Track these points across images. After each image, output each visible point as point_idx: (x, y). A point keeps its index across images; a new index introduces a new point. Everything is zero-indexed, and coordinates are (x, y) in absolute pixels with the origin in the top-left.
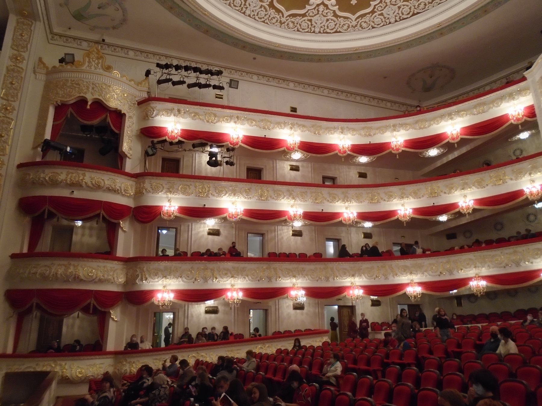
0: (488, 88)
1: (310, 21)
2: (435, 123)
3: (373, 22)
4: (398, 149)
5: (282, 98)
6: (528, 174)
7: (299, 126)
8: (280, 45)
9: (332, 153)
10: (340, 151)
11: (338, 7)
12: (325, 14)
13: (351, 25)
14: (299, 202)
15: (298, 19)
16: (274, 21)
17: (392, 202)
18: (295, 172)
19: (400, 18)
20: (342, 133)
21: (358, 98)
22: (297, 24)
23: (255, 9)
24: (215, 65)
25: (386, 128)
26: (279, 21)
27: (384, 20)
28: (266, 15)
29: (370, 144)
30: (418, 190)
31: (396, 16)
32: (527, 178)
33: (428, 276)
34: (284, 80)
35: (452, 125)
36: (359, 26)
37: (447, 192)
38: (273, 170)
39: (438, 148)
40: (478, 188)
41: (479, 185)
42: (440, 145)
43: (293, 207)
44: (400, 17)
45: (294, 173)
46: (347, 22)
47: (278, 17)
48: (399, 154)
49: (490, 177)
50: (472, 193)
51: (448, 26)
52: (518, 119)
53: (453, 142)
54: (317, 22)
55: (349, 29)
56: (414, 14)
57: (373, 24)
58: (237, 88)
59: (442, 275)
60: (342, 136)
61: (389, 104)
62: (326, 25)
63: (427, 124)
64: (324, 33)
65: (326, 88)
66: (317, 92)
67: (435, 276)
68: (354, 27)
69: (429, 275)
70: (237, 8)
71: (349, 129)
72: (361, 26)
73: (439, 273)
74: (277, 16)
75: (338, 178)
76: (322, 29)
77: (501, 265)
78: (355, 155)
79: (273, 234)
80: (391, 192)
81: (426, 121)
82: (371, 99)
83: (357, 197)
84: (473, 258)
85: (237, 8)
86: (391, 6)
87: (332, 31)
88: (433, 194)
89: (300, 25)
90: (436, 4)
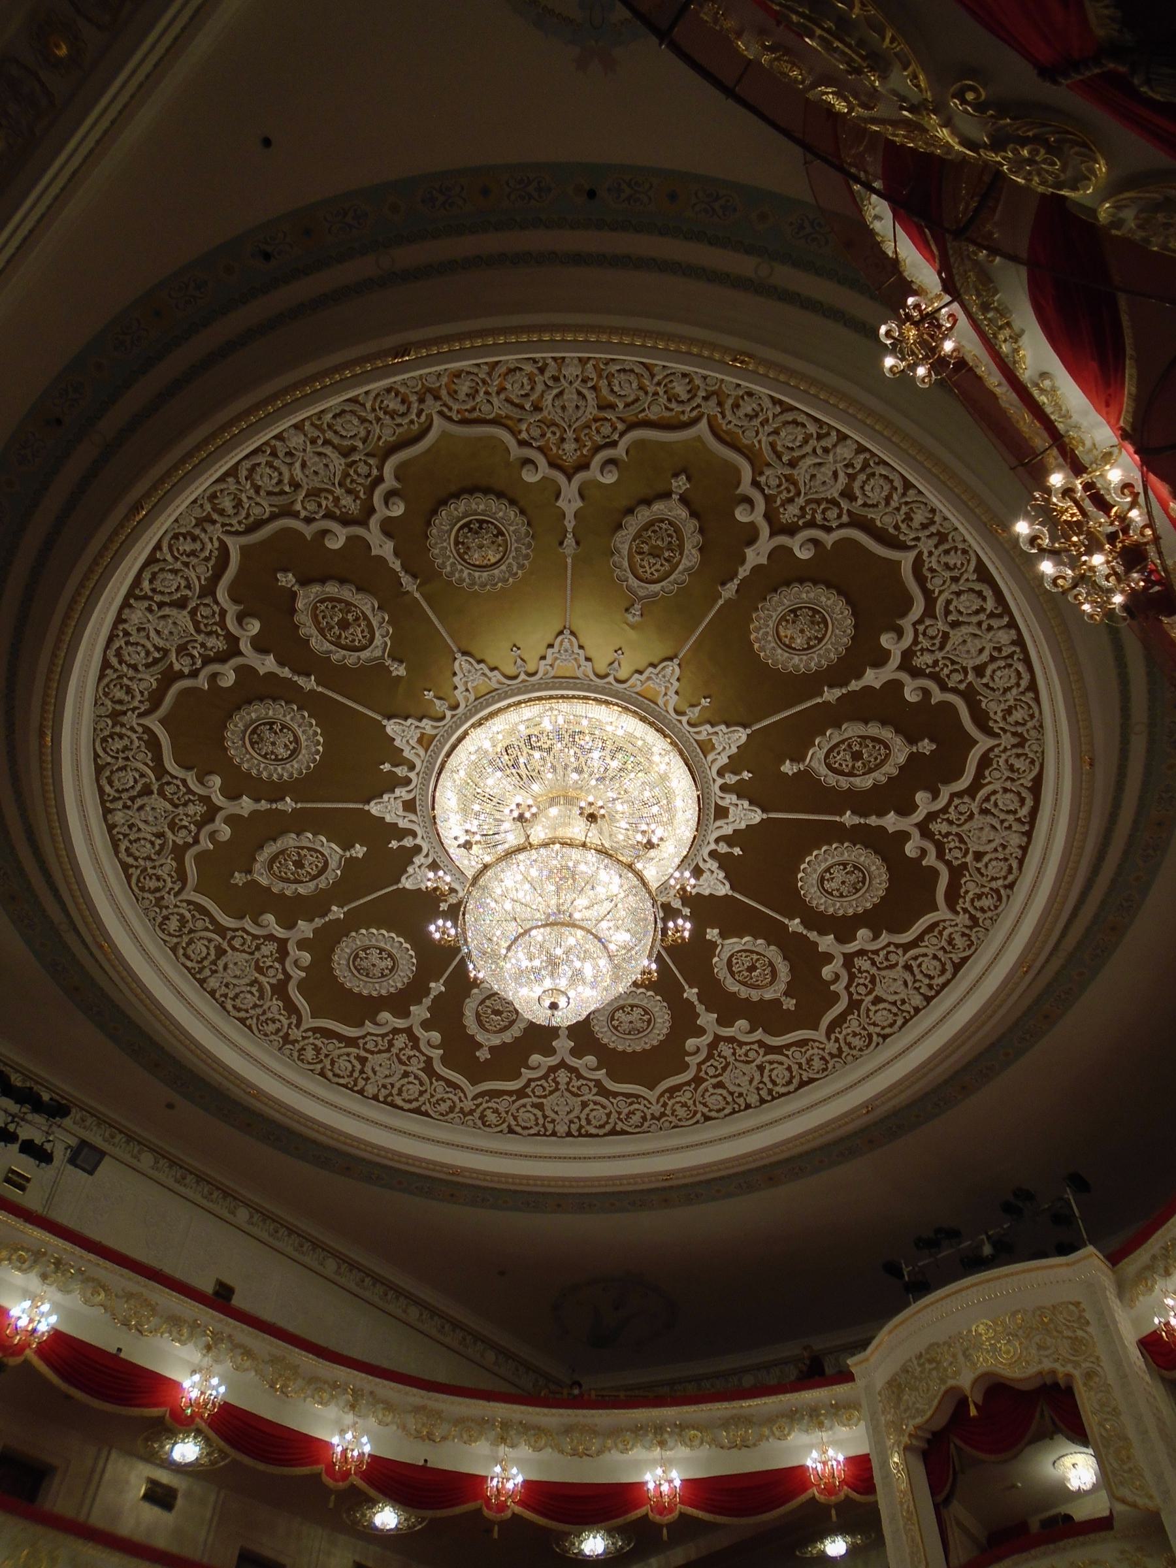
0: (748, 1381)
1: (363, 1061)
3: (515, 1118)
5: (203, 1244)
7: (235, 1346)
8: (260, 1095)
11: (441, 1052)
12: (404, 1058)
13: (459, 1105)
15: (333, 1048)
16: (271, 1028)
19: (579, 1130)
21: (414, 1312)
22: (326, 1056)
23: (235, 981)
24: (54, 1083)
25: (483, 1425)
26: (281, 1034)
27: (541, 1121)
28: (255, 1006)
29: (424, 1469)
31: (571, 1122)
34: (226, 1194)
36: (477, 1114)
39: (610, 1533)
42: (620, 1521)
44: (581, 1127)
46: (451, 1096)
47: (285, 1022)
48: (503, 1524)
51: (686, 1185)
52: (830, 1490)
53: (657, 1518)
54: (377, 1068)
56: (613, 1132)
58: (91, 1173)
60: (349, 1418)
61: (491, 1356)
62: (398, 1085)
64: (385, 1102)
66: (307, 1259)
70: (189, 964)
72: (482, 1117)
74: (282, 1018)
76: (384, 1092)
78: (372, 1493)
81: (593, 1432)
85: (189, 964)
86: (567, 1094)
87: (407, 1106)
89: (333, 1063)
90: (667, 1124)
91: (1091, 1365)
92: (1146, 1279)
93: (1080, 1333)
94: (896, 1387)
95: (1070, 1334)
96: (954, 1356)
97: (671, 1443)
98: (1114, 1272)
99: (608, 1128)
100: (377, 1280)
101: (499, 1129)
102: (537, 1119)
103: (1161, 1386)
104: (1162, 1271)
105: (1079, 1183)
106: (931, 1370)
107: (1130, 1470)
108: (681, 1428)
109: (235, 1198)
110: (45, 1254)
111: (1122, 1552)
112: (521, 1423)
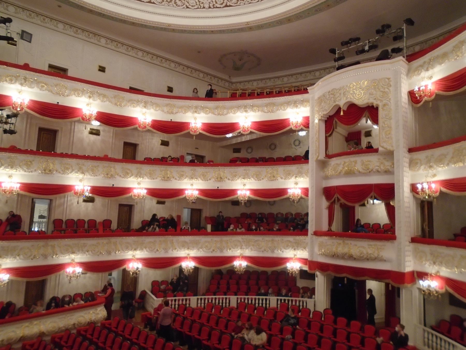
3: (188, 3)
4: (195, 131)
7: (100, 95)
9: (132, 127)
10: (139, 126)
14: (89, 177)
18: (95, 136)
20: (145, 107)
25: (188, 108)
27: (198, 3)
29: (171, 122)
30: (207, 173)
32: (293, 180)
33: (203, 252)
34: (95, 34)
35: (246, 117)
37: (231, 179)
38: (70, 133)
40: (256, 180)
43: (80, 181)
45: (93, 137)
49: (267, 172)
50: (250, 183)
55: (163, 3)
56: (226, 6)
57: (188, 5)
59: (214, 252)
60: (144, 110)
61: (201, 75)
63: (225, 111)
65: (141, 50)
68: (169, 2)
69: (204, 251)
71: (153, 104)
72: (175, 3)
73: (211, 250)
75: (140, 145)
79: (62, 200)
81: (224, 108)
82: (185, 68)
83: (150, 174)
88: (220, 179)
93: (386, 90)
94: (321, 100)
95: (382, 90)
96: (340, 94)
97: (249, 111)
98: (408, 65)
99: (224, 5)
100: (158, 56)
101: (183, 7)
102: (196, 3)
103: (411, 108)
104: (425, 68)
105: (410, 22)
107: (388, 138)
108: (252, 106)
109: (99, 35)
110: (19, 76)
111: (379, 159)
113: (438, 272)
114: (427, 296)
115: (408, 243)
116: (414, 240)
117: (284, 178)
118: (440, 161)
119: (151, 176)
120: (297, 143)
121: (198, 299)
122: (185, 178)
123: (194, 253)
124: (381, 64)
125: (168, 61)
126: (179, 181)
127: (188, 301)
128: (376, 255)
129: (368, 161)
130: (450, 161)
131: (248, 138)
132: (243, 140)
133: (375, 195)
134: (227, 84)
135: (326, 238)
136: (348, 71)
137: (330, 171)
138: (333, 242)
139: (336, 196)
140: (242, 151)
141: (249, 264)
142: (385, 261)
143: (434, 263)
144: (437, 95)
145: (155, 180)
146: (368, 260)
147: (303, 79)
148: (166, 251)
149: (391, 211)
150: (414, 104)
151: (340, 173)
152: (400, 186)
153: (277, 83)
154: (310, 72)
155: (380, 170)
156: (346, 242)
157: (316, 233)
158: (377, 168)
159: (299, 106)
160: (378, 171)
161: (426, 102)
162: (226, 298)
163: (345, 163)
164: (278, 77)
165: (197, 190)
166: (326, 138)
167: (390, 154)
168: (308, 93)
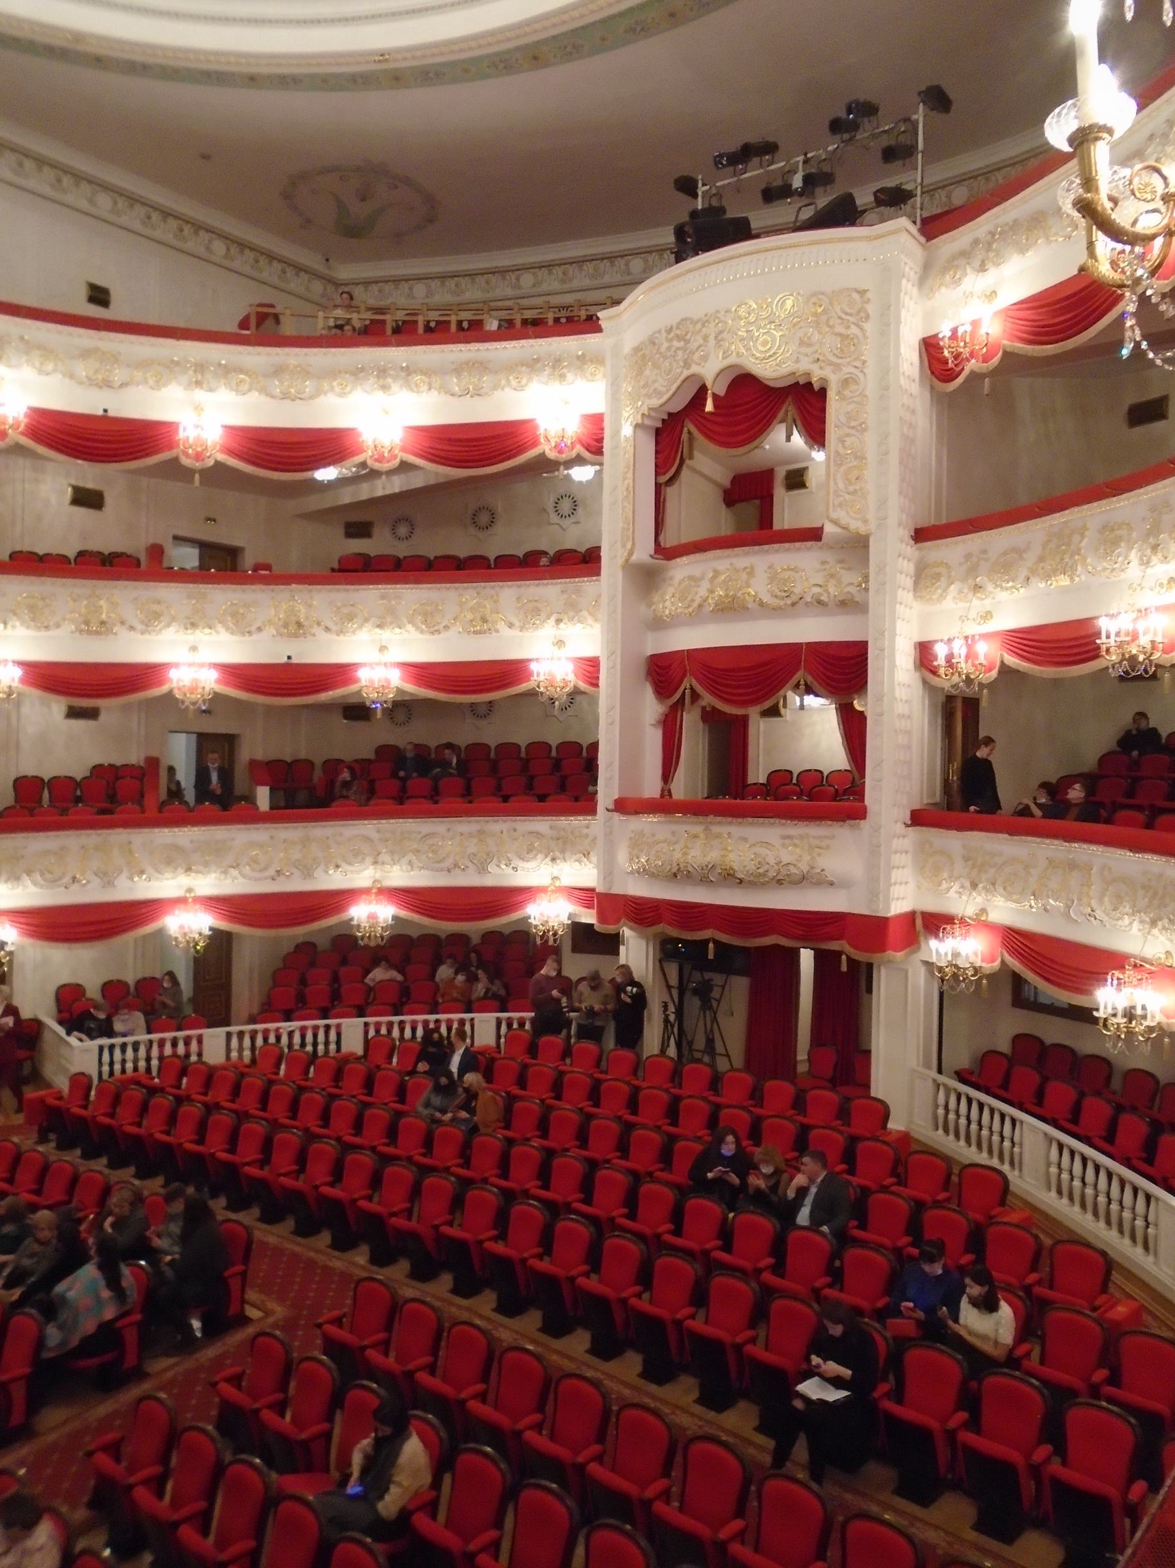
2: (332, 389)
4: (198, 456)
6: (552, 621)
17: (160, 637)
25: (172, 367)
29: (105, 418)
33: (241, 880)
35: (383, 409)
37: (334, 628)
40: (422, 632)
41: (425, 622)
59: (281, 878)
61: (219, 247)
67: (256, 880)
69: (244, 876)
77: (441, 865)
80: (159, 603)
81: (305, 372)
82: (155, 216)
83: (32, 608)
84: (374, 835)
88: (297, 629)
91: (853, 370)
92: (957, 267)
93: (854, 330)
94: (643, 356)
95: (840, 329)
96: (706, 338)
103: (927, 395)
104: (977, 263)
105: (938, 99)
106: (678, 349)
107: (855, 492)
111: (824, 563)
112: (220, 364)
113: (983, 911)
114: (950, 985)
115: (900, 828)
116: (918, 819)
117: (517, 624)
118: (1005, 568)
119: (37, 616)
120: (566, 506)
121: (229, 1035)
122: (168, 625)
123: (209, 883)
124: (840, 240)
125: (84, 186)
126: (147, 636)
127: (194, 1046)
128: (805, 868)
129: (789, 569)
130: (1033, 571)
131: (396, 485)
132: (380, 493)
133: (810, 679)
134: (317, 287)
135: (653, 819)
136: (732, 258)
137: (668, 601)
138: (673, 833)
139: (686, 684)
140: (376, 531)
141: (403, 913)
142: (832, 884)
143: (974, 886)
144: (1007, 355)
145: (50, 633)
146: (780, 882)
147: (587, 282)
148: (108, 881)
149: (854, 728)
150: (937, 383)
151: (700, 606)
152: (883, 650)
153: (498, 293)
154: (611, 258)
155: (824, 598)
156: (716, 829)
157: (622, 806)
158: (817, 590)
159: (570, 376)
160: (820, 602)
161: (975, 376)
162: (328, 1027)
163: (717, 573)
164: (502, 272)
165: (216, 666)
166: (658, 488)
167: (857, 547)
168: (599, 330)
